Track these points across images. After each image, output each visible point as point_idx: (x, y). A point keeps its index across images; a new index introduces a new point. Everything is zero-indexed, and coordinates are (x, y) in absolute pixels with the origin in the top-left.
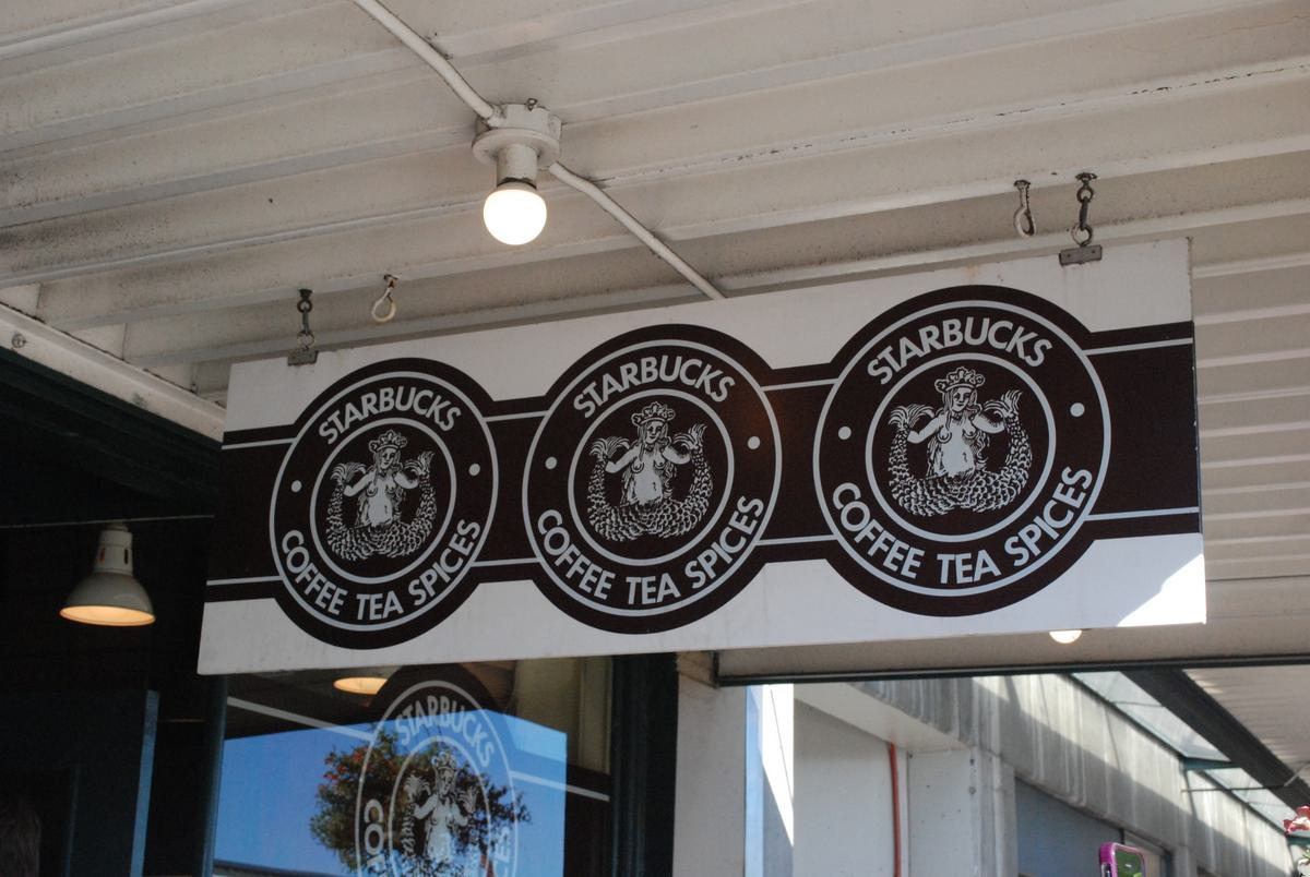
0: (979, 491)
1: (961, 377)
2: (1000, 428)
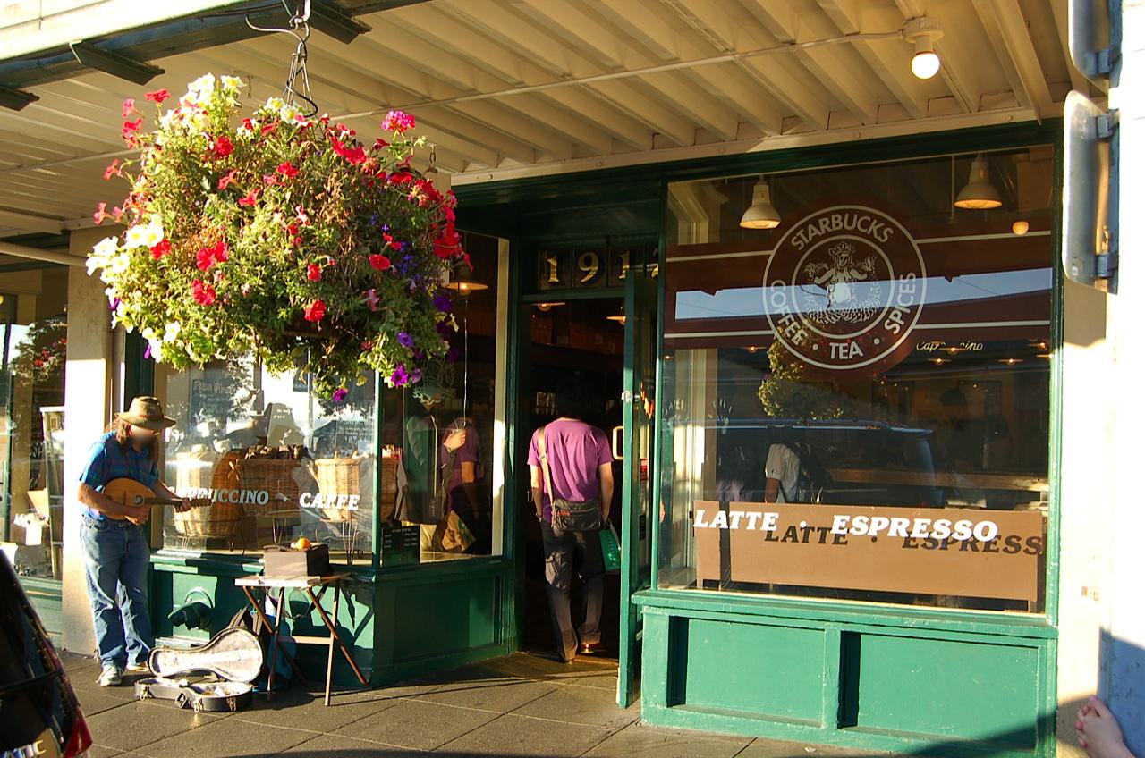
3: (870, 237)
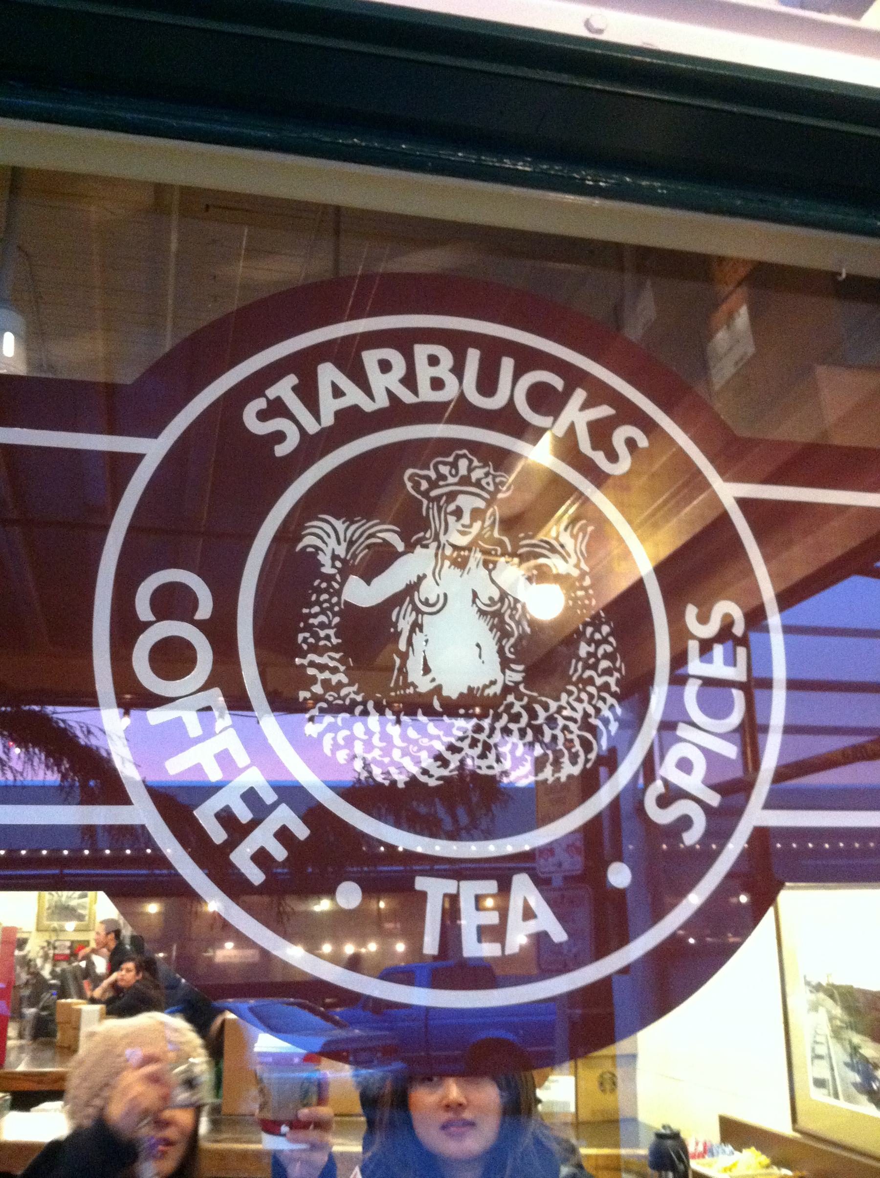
1: (463, 471)
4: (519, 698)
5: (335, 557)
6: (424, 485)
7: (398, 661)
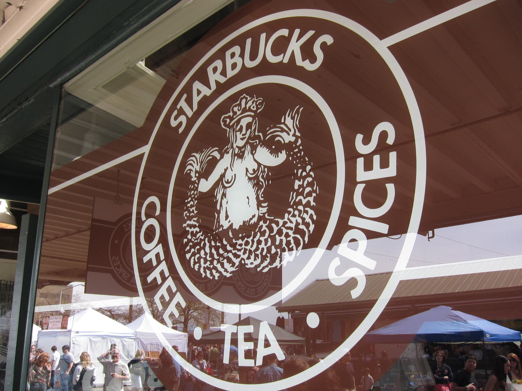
0: (263, 245)
2: (282, 157)
3: (290, 69)
4: (265, 222)
5: (196, 172)
6: (228, 120)
7: (216, 215)
